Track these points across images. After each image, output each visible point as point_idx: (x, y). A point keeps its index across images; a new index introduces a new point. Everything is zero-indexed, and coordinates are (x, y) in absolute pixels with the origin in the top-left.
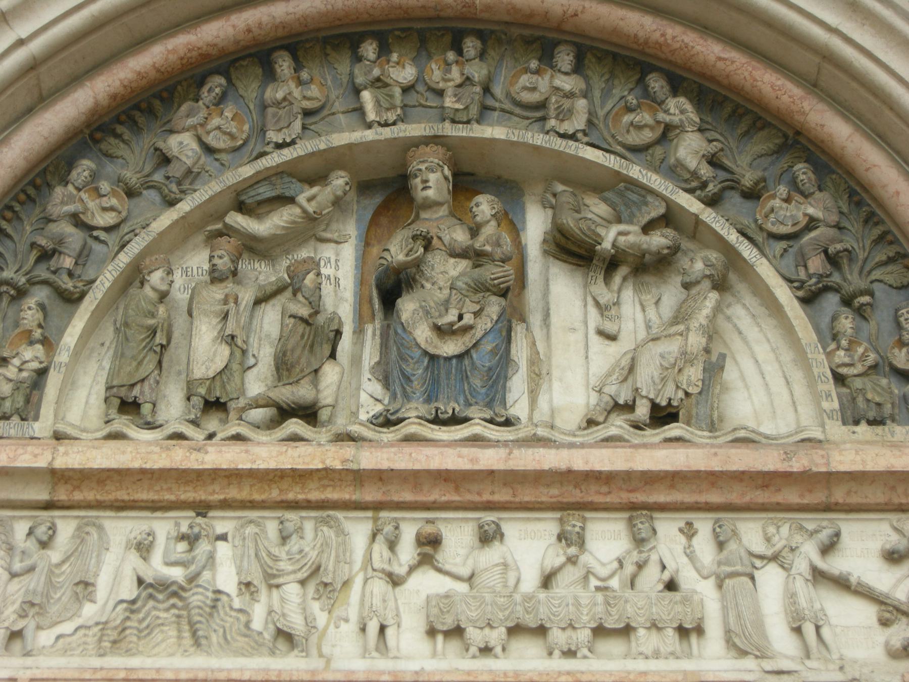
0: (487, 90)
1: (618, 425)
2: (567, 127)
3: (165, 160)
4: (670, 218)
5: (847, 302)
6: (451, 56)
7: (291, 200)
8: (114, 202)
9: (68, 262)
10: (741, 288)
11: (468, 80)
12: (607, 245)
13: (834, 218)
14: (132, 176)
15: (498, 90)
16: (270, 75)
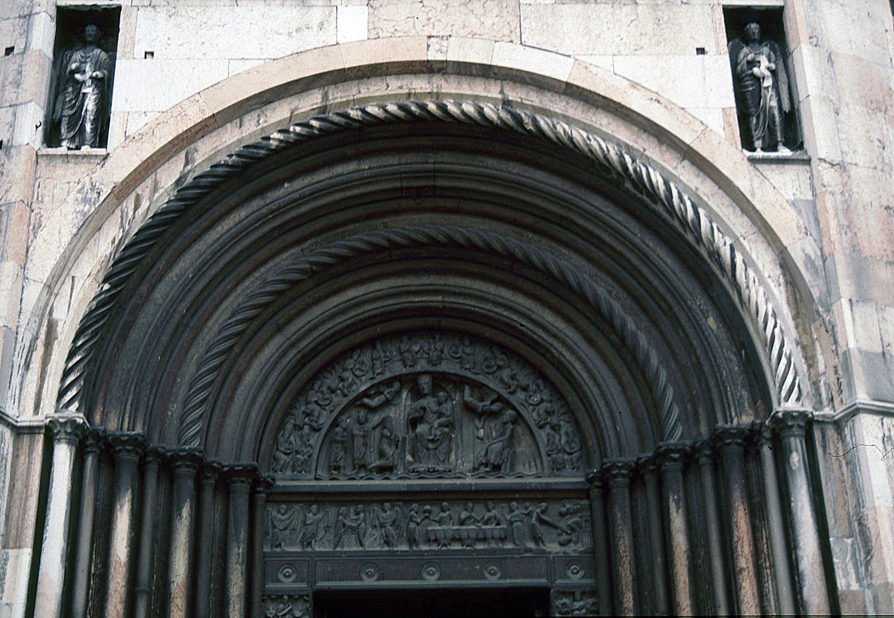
0: (442, 351)
1: (483, 469)
2: (467, 366)
3: (342, 380)
4: (500, 399)
5: (552, 428)
6: (431, 340)
7: (382, 393)
8: (328, 396)
9: (315, 418)
10: (520, 421)
11: (436, 349)
12: (480, 410)
13: (549, 398)
14: (333, 386)
15: (445, 351)
16: (374, 347)
